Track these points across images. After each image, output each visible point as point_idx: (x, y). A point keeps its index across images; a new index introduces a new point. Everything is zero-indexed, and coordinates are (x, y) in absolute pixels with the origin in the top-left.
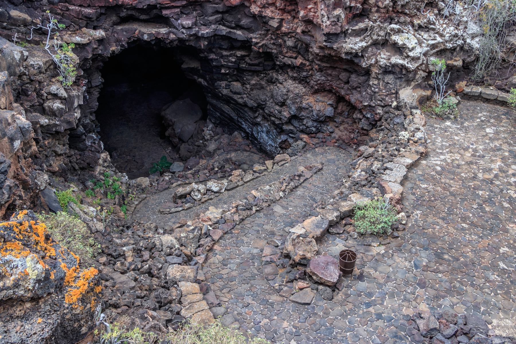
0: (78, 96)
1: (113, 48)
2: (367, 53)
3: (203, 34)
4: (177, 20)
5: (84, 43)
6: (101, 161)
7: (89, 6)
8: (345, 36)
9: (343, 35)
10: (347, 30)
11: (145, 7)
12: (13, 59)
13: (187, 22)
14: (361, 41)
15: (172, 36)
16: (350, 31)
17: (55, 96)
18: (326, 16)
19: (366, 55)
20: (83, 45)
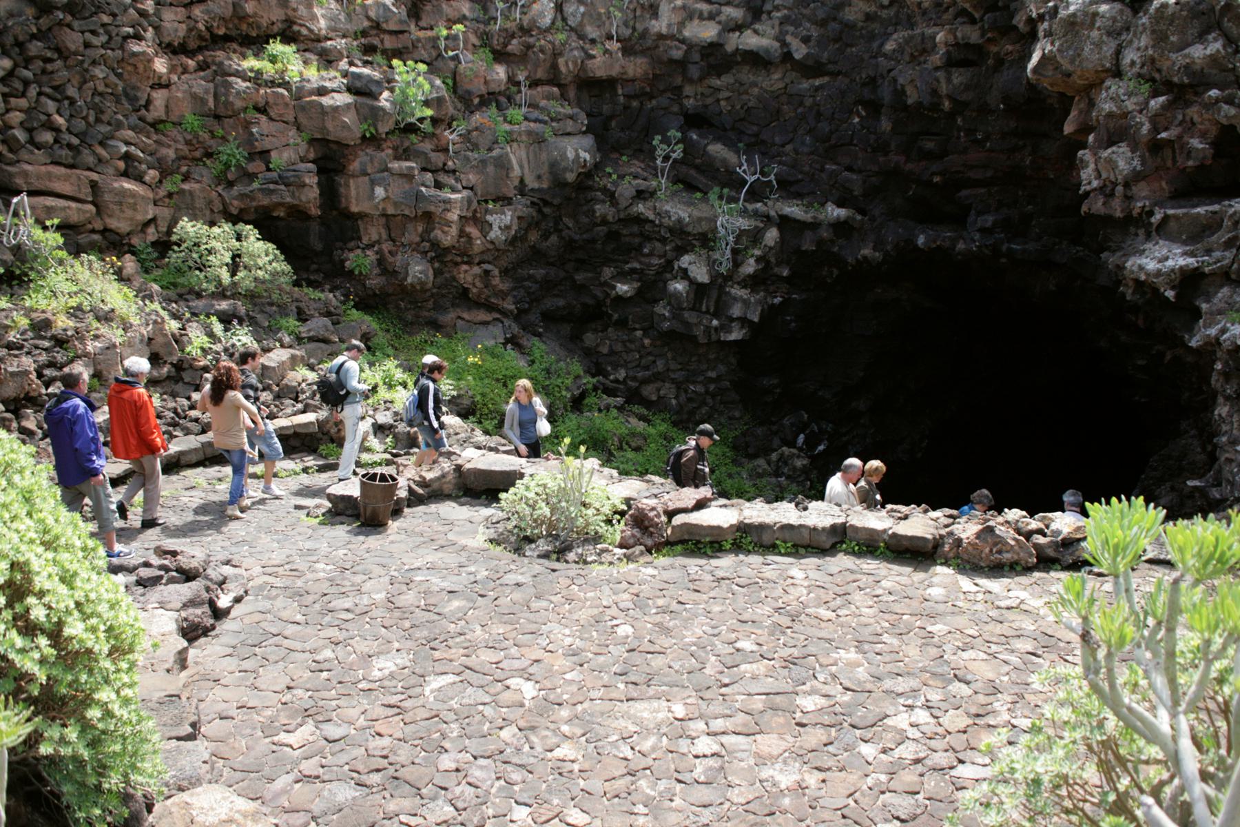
0: (746, 303)
1: (866, 252)
2: (1208, 301)
3: (1009, 249)
4: (979, 213)
5: (799, 218)
6: (774, 456)
7: (860, 172)
8: (1148, 237)
9: (1141, 232)
10: (1151, 213)
11: (936, 179)
12: (564, 156)
13: (989, 220)
14: (1192, 254)
15: (961, 246)
16: (1157, 217)
17: (685, 275)
18: (1092, 166)
19: (1204, 306)
20: (799, 221)
